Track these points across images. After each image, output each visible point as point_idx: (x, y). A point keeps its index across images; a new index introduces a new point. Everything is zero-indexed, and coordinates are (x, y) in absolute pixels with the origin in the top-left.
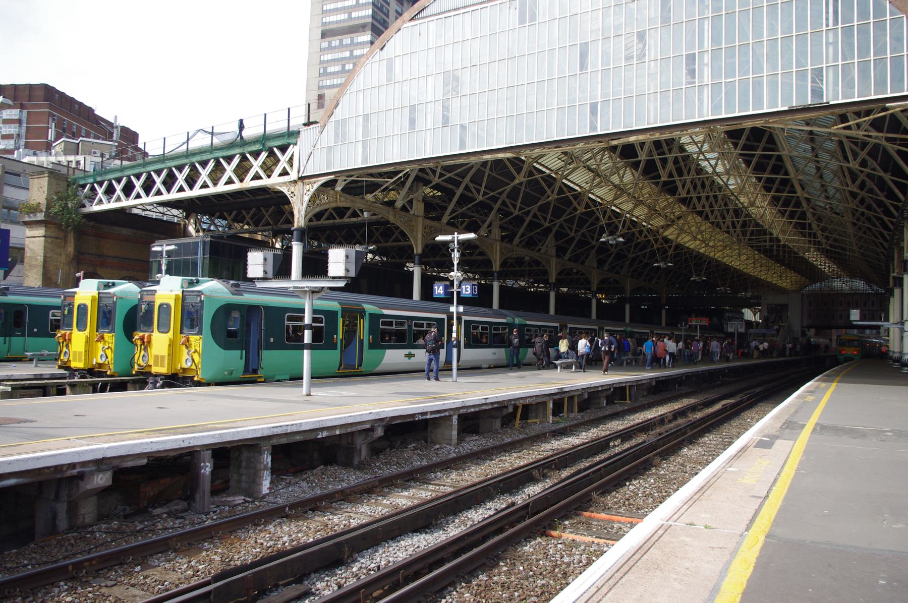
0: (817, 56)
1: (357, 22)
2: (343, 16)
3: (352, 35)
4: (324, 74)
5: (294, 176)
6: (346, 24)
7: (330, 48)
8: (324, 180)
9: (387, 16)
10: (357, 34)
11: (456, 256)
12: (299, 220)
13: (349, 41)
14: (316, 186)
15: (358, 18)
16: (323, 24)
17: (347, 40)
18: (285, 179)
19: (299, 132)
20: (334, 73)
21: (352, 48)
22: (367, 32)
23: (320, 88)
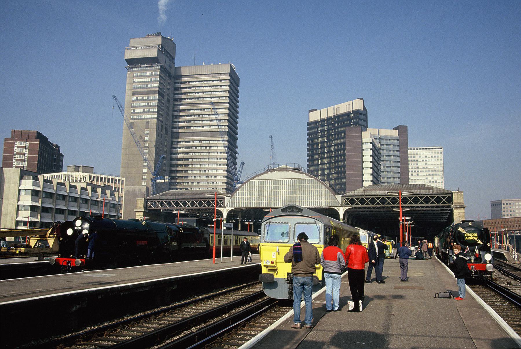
13: (147, 98)
14: (229, 210)
15: (152, 87)
20: (139, 113)
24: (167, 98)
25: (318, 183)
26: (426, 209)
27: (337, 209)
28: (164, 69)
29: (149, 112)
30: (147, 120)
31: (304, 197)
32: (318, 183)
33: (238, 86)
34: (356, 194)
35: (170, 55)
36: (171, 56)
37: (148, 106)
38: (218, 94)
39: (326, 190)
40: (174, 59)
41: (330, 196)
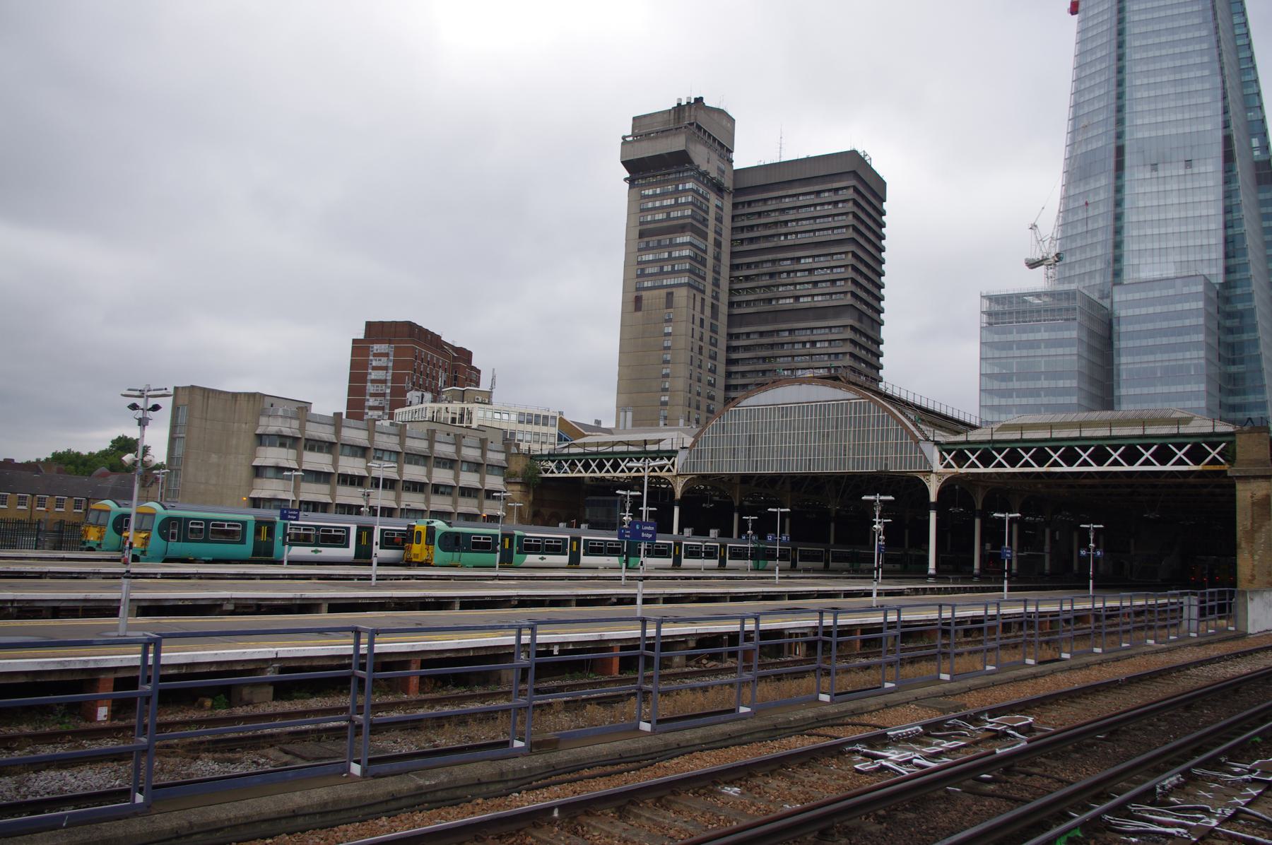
0: (887, 454)
1: (675, 222)
2: (660, 216)
3: (671, 236)
4: (642, 275)
5: (675, 473)
6: (665, 224)
7: (647, 249)
8: (691, 476)
9: (707, 213)
10: (676, 235)
11: (750, 525)
12: (678, 495)
15: (677, 218)
16: (641, 223)
17: (665, 240)
18: (670, 474)
19: (676, 452)
20: (652, 275)
21: (670, 249)
22: (687, 234)
23: (638, 289)
24: (715, 239)
25: (878, 412)
26: (1197, 480)
27: (922, 478)
28: (705, 174)
29: (673, 272)
30: (669, 290)
31: (845, 447)
32: (878, 412)
33: (882, 199)
34: (970, 438)
35: (719, 143)
36: (722, 146)
37: (670, 258)
38: (830, 222)
39: (897, 429)
40: (732, 152)
41: (906, 443)
